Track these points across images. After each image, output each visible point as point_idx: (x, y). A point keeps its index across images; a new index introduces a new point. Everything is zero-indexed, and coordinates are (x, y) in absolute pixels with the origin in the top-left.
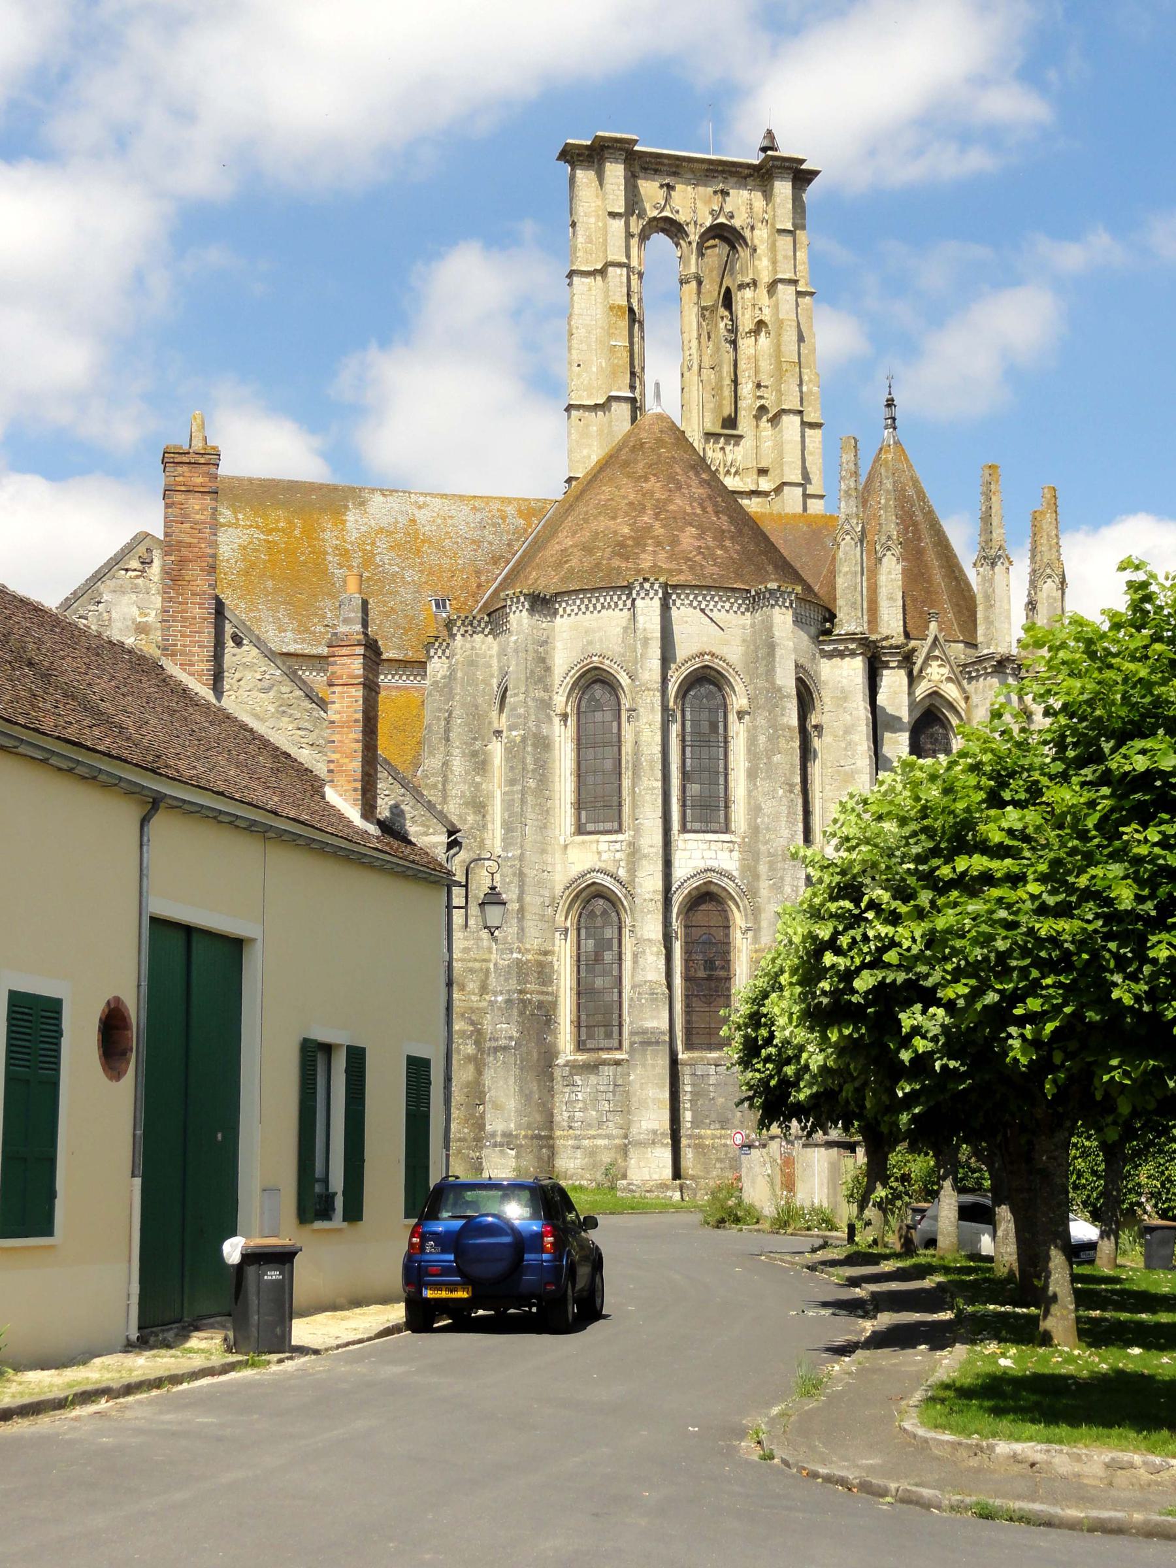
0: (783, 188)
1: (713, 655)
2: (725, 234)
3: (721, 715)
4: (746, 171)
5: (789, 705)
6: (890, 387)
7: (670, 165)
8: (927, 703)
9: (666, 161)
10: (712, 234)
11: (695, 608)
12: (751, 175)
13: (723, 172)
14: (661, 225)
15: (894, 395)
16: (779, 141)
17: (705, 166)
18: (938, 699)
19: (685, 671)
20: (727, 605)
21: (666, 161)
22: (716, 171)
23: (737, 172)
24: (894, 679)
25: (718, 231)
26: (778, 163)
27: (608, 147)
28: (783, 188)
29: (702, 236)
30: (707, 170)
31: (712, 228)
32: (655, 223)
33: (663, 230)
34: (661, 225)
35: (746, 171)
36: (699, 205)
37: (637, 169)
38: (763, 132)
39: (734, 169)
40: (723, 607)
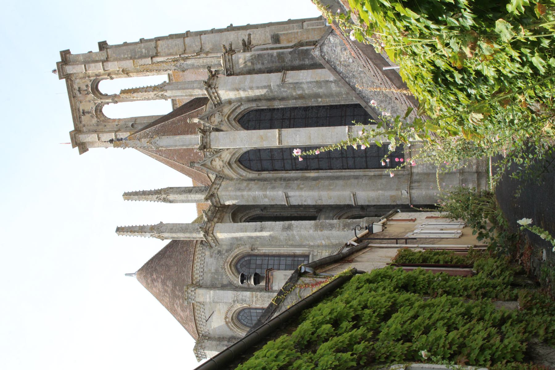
0: (69, 69)
1: (226, 318)
2: (95, 86)
3: (252, 311)
4: (69, 81)
5: (240, 297)
6: (105, 142)
7: (76, 113)
8: (234, 166)
9: (75, 115)
10: (96, 92)
11: (206, 324)
12: (70, 80)
13: (72, 91)
14: (99, 113)
15: (109, 140)
16: (53, 69)
17: (72, 99)
18: (232, 160)
19: (236, 329)
20: (202, 310)
21: (75, 115)
22: (73, 93)
23: (71, 84)
24: (224, 198)
25: (95, 90)
26: (61, 73)
27: (76, 142)
28: (69, 69)
29: (98, 97)
30: (74, 97)
31: (94, 93)
32: (99, 116)
33: (101, 111)
34: (99, 113)
35: (69, 81)
36: (87, 99)
37: (81, 125)
38: (53, 74)
39: (70, 87)
40: (203, 312)
